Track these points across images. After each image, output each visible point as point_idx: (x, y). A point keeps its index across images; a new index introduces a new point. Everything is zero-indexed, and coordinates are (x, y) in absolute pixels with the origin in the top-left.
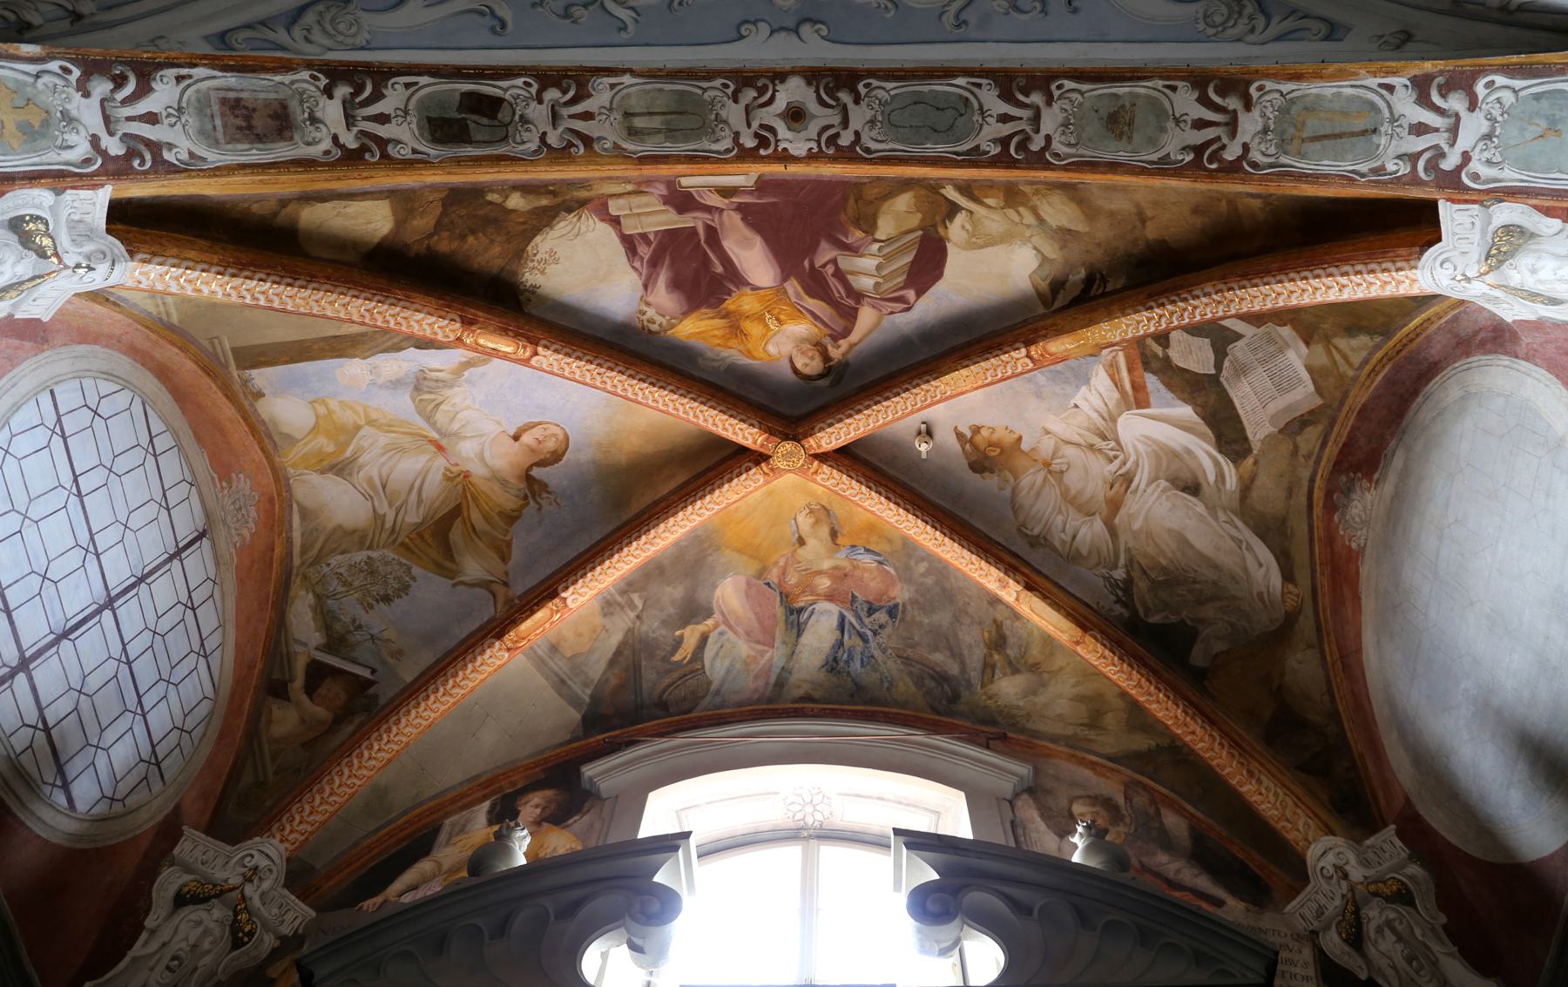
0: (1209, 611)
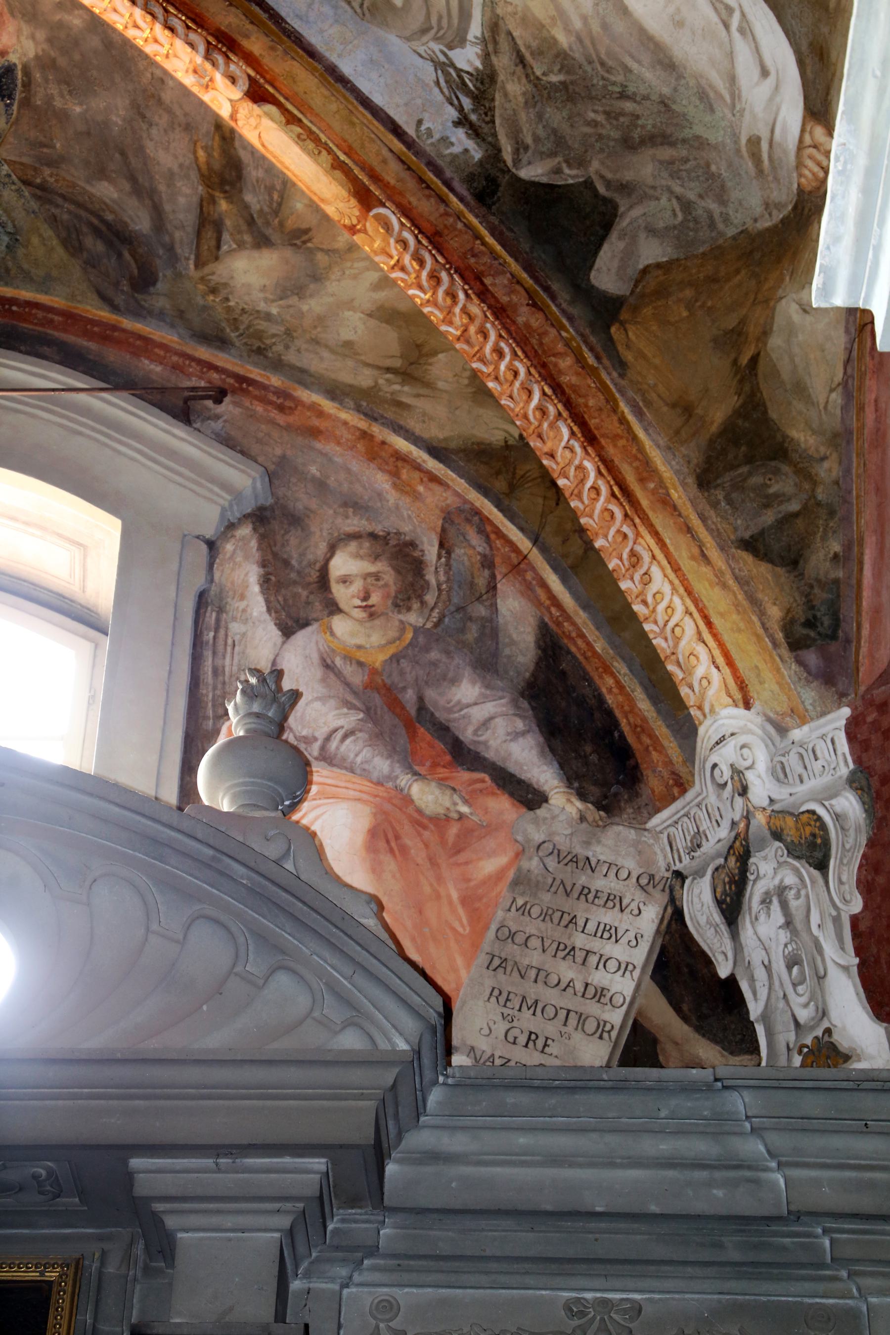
0: (644, 168)
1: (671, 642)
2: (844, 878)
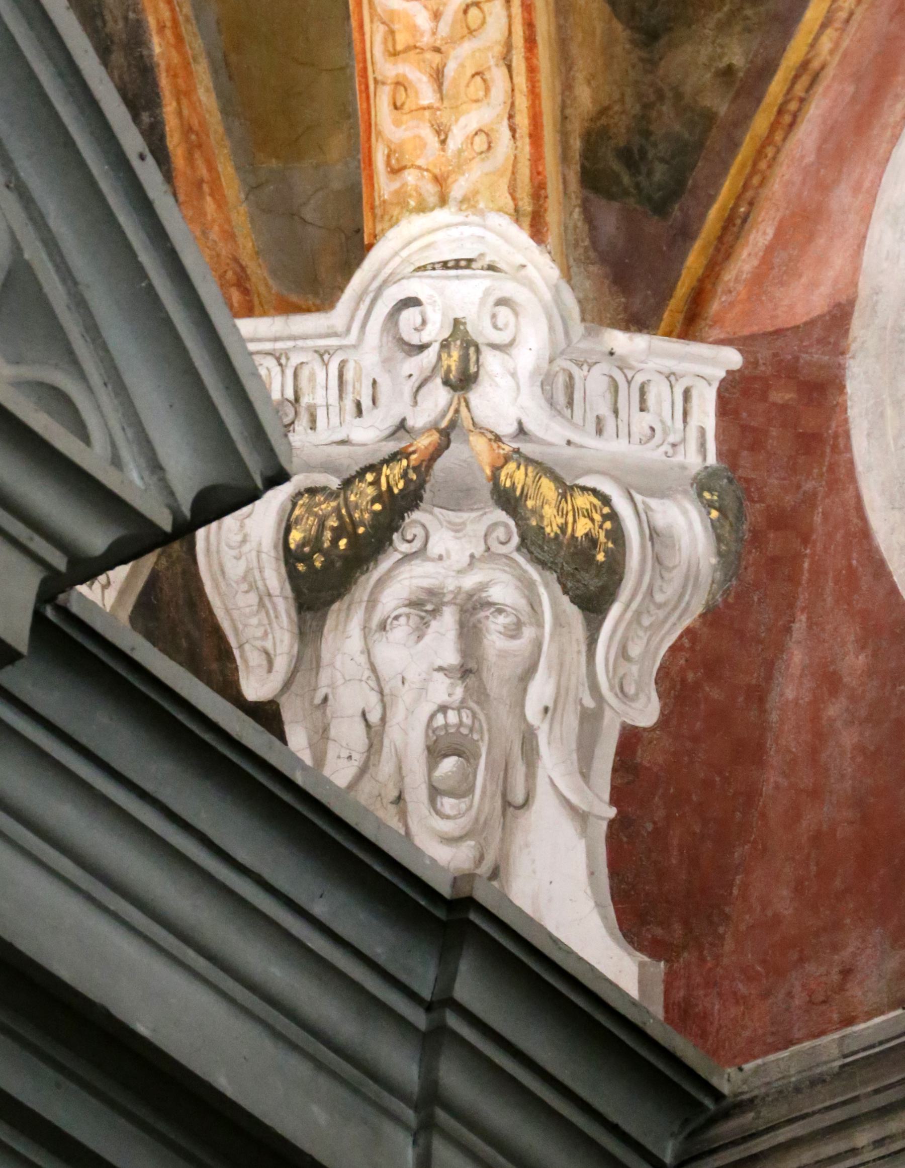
1: (444, 28)
2: (635, 650)
